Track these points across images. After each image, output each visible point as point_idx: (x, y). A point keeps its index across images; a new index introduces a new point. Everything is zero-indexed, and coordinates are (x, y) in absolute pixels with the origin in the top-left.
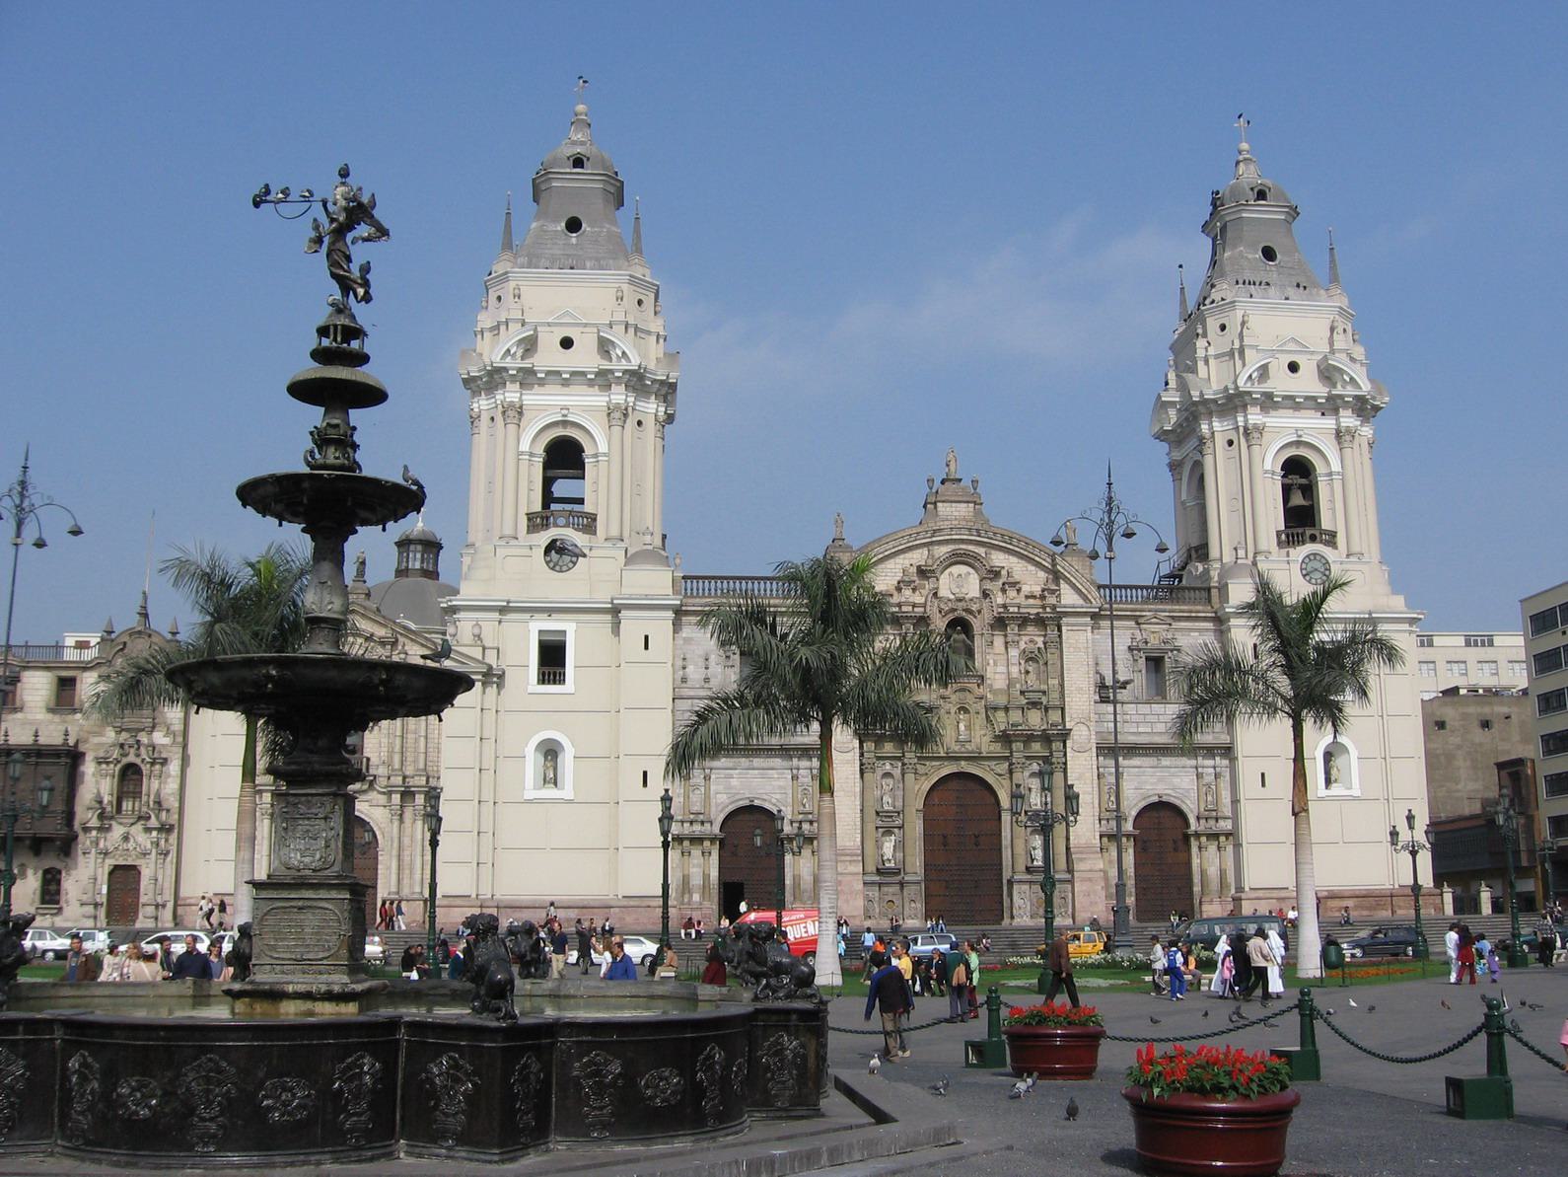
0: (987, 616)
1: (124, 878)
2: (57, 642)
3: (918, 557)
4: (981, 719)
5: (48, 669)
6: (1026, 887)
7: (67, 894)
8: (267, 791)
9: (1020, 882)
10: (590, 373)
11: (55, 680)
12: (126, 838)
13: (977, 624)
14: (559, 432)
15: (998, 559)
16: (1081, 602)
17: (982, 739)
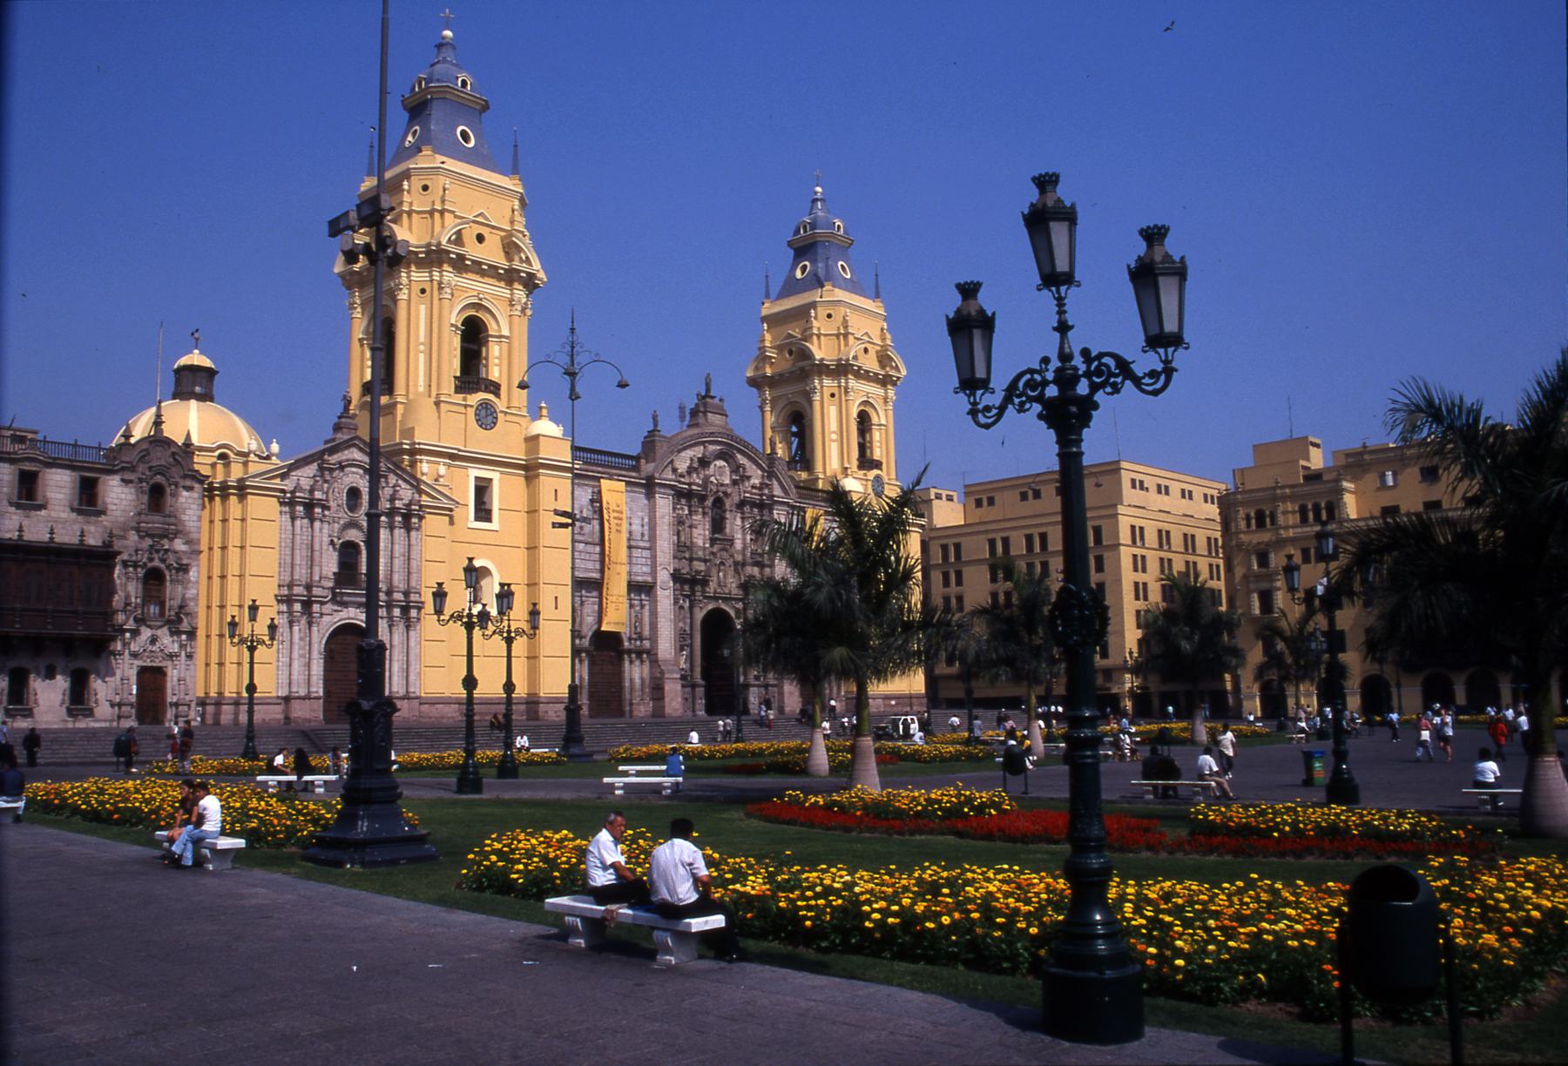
0: (736, 499)
1: (152, 679)
2: (76, 441)
3: (698, 452)
4: (731, 572)
5: (72, 468)
6: (756, 689)
7: (96, 694)
8: (297, 601)
9: (754, 686)
10: (502, 269)
11: (78, 479)
12: (153, 640)
13: (728, 503)
14: (472, 312)
15: (741, 459)
16: (782, 495)
17: (732, 584)
